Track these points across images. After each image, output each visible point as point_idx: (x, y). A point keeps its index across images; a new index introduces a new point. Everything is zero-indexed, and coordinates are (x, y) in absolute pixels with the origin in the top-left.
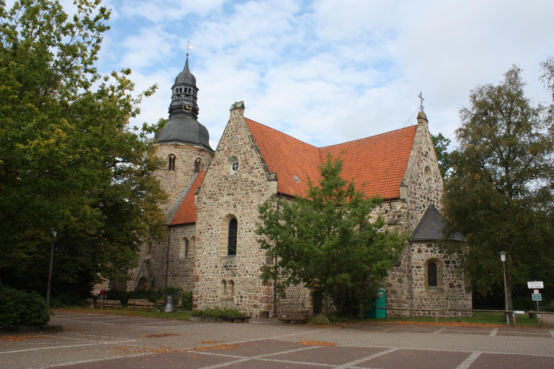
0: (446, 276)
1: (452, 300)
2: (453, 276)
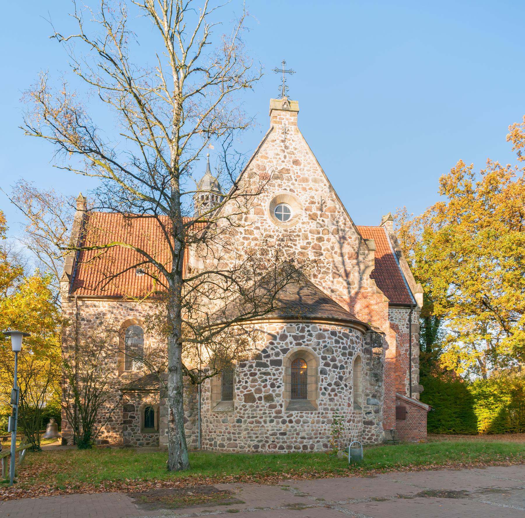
0: (239, 382)
1: (252, 423)
2: (254, 381)
